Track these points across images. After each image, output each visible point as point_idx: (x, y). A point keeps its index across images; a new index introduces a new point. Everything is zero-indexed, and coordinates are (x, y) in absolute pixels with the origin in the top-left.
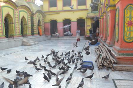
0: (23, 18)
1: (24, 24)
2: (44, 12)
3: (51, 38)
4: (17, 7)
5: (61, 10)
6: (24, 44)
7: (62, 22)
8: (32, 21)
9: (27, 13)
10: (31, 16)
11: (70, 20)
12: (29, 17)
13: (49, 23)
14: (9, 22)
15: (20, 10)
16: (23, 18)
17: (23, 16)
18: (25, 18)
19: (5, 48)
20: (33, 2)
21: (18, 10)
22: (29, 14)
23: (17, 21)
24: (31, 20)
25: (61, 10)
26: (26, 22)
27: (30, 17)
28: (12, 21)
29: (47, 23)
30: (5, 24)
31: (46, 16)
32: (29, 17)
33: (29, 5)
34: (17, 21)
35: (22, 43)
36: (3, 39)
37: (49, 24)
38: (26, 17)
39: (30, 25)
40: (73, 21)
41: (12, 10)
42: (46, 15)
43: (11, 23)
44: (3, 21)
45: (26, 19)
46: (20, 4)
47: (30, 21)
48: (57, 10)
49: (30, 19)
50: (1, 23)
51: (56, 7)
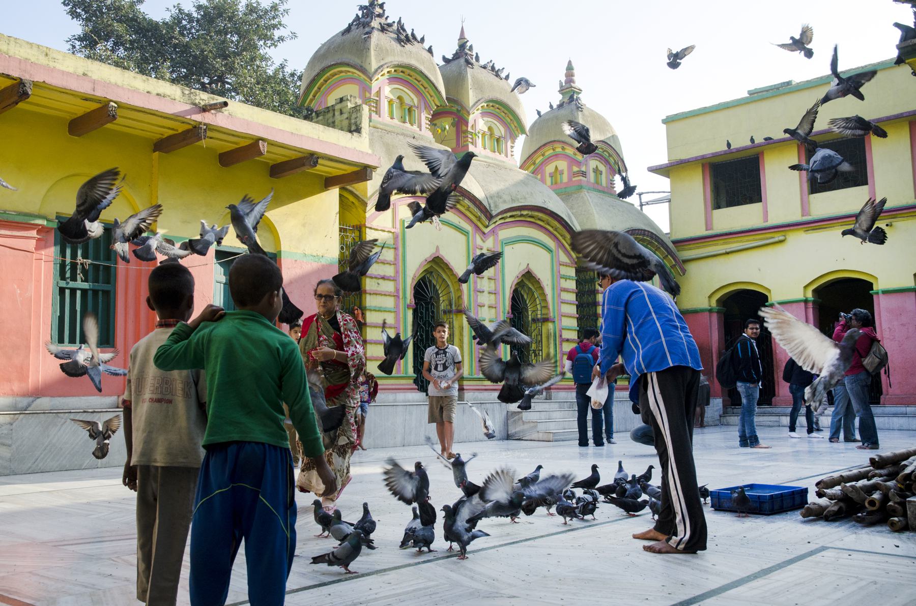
0: (528, 278)
1: (535, 320)
2: (674, 242)
3: (725, 413)
4: (490, 217)
5: (796, 216)
6: (512, 430)
7: (806, 301)
8: (585, 299)
9: (549, 250)
10: (578, 271)
11: (869, 285)
12: (566, 278)
13: (710, 311)
14: (443, 306)
15: (504, 234)
16: (528, 278)
17: (522, 268)
18: (537, 282)
19: (399, 439)
20: (597, 182)
21: (493, 231)
22: (563, 258)
23: (485, 299)
24: (580, 294)
25: (797, 217)
26: (546, 307)
27: (572, 272)
28: (460, 297)
29: (695, 312)
30: (415, 312)
31: (692, 268)
32: (566, 278)
33: (571, 208)
34: (485, 299)
35: (506, 424)
36: (401, 396)
37: (715, 317)
38: (544, 274)
39: (574, 323)
40: (885, 292)
41: (462, 238)
42: (685, 261)
43: (454, 308)
44: (405, 297)
45: (544, 294)
46: (505, 202)
47: (572, 297)
48: (766, 219)
49: (572, 285)
50: (397, 306)
51: (759, 200)
